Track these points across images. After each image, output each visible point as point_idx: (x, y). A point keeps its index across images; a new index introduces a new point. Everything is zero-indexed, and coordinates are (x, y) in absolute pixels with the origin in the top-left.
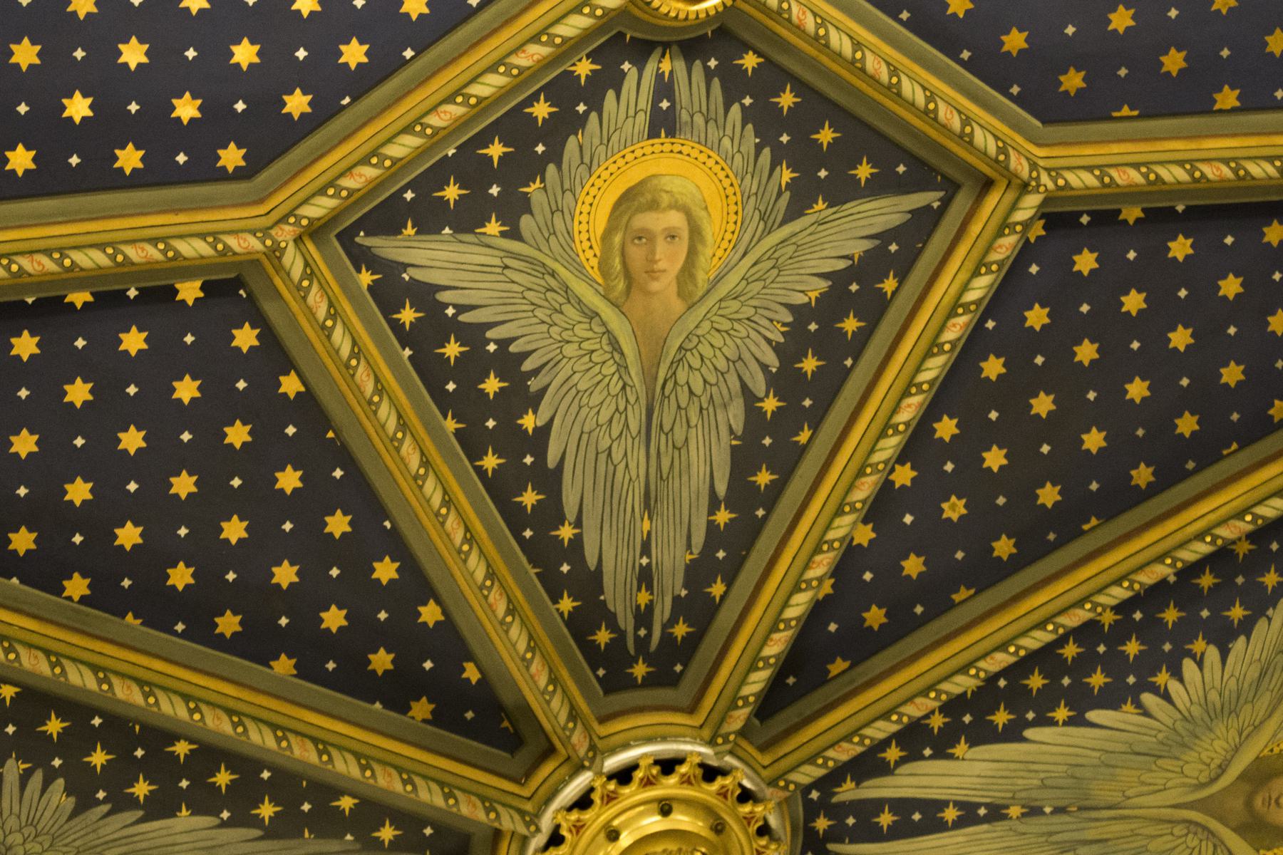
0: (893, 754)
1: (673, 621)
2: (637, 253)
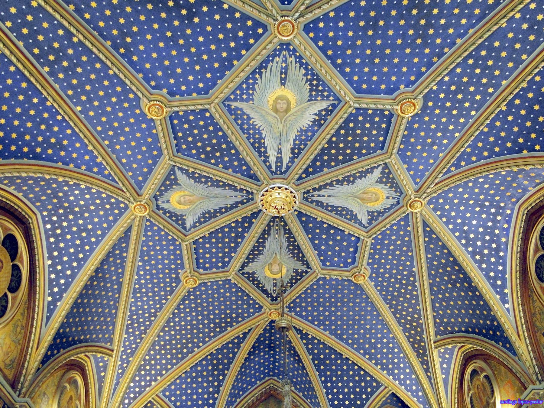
0: (268, 164)
2: (187, 202)
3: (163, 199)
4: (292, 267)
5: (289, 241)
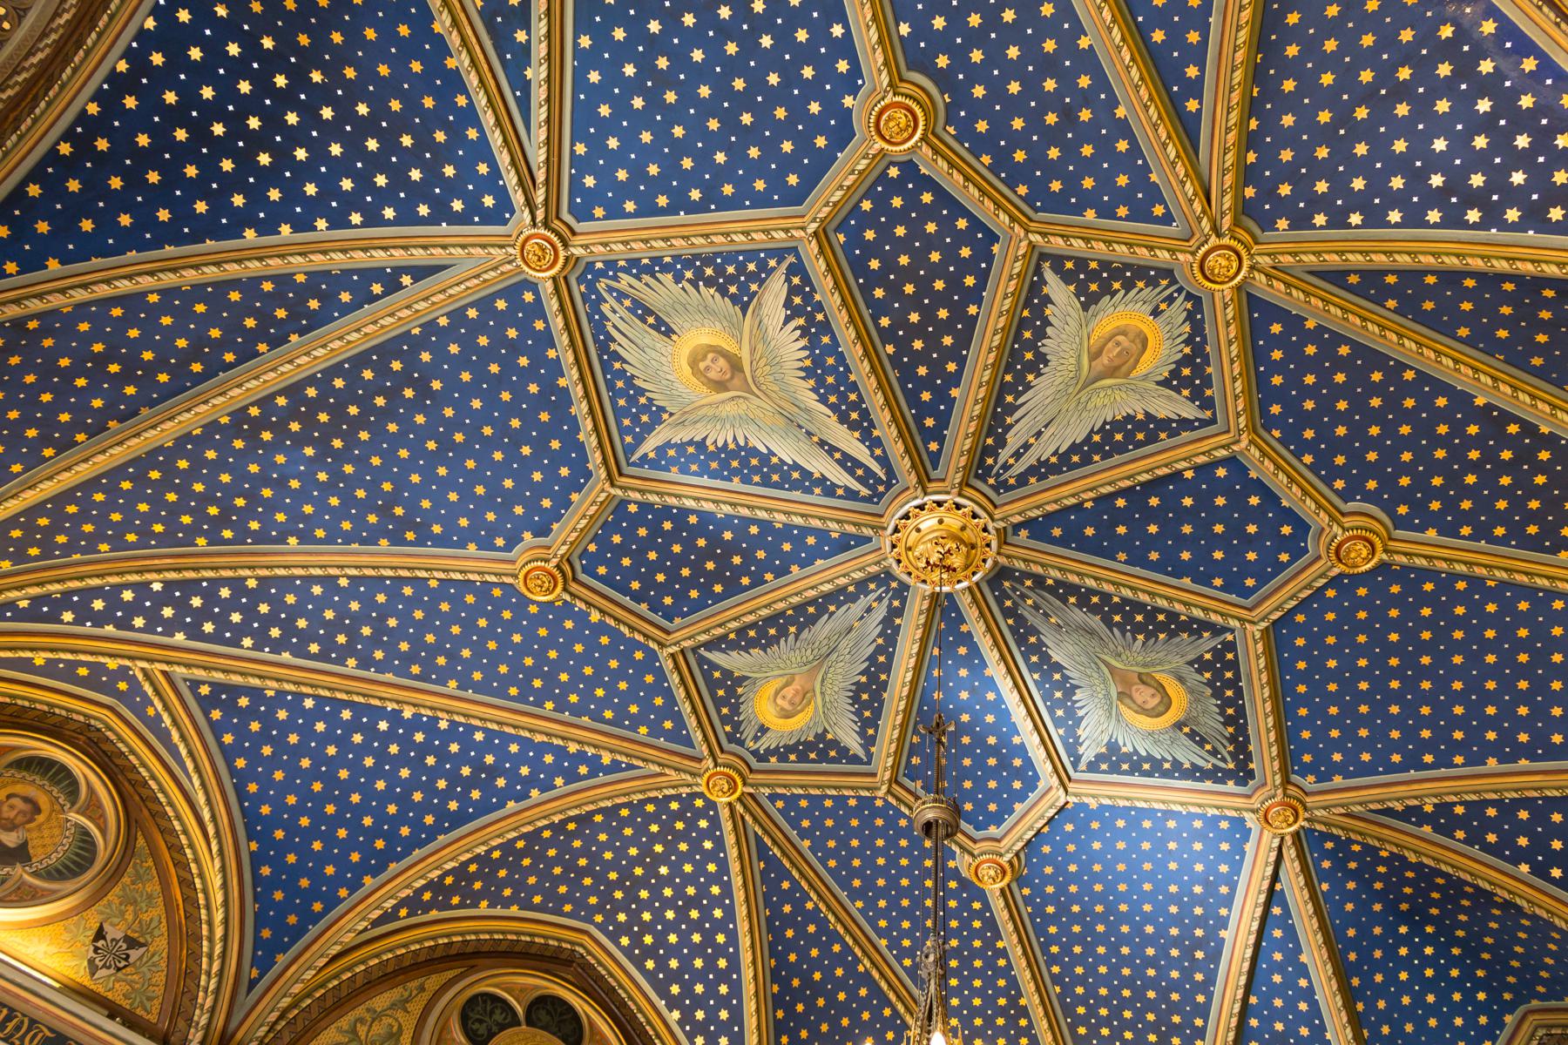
0: (840, 492)
1: (873, 591)
2: (797, 700)
3: (748, 733)
4: (1178, 662)
5: (1094, 609)
